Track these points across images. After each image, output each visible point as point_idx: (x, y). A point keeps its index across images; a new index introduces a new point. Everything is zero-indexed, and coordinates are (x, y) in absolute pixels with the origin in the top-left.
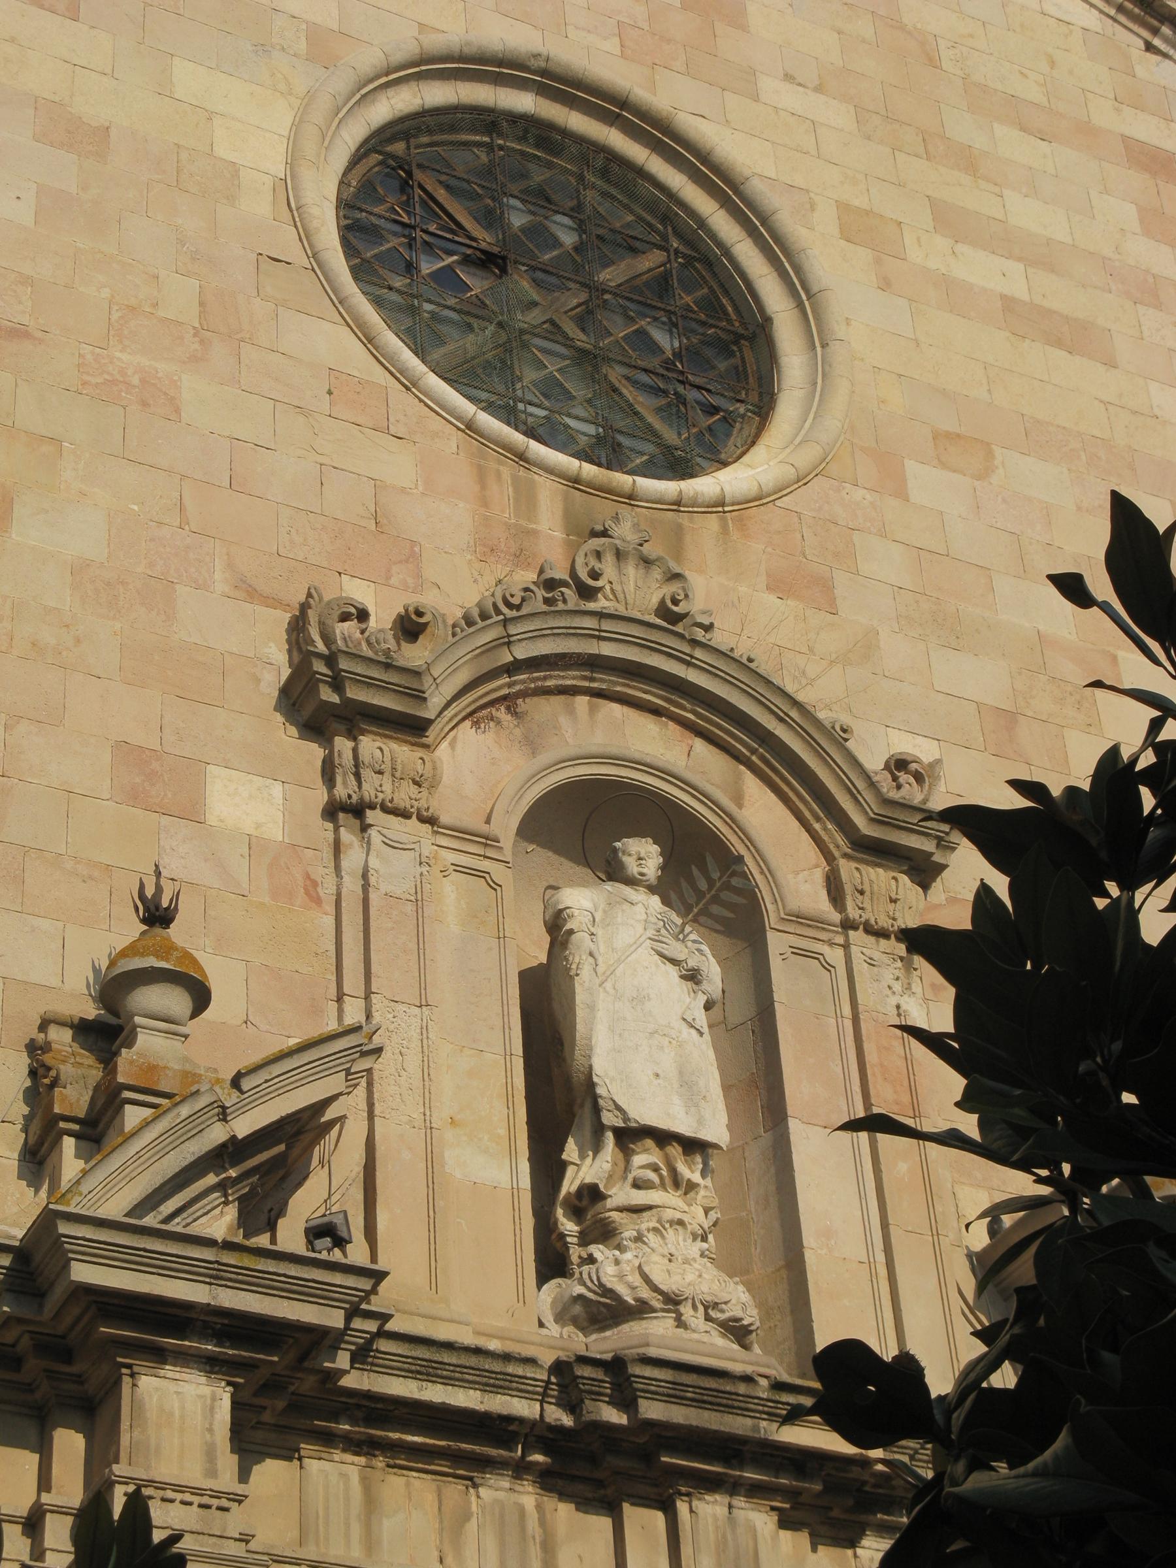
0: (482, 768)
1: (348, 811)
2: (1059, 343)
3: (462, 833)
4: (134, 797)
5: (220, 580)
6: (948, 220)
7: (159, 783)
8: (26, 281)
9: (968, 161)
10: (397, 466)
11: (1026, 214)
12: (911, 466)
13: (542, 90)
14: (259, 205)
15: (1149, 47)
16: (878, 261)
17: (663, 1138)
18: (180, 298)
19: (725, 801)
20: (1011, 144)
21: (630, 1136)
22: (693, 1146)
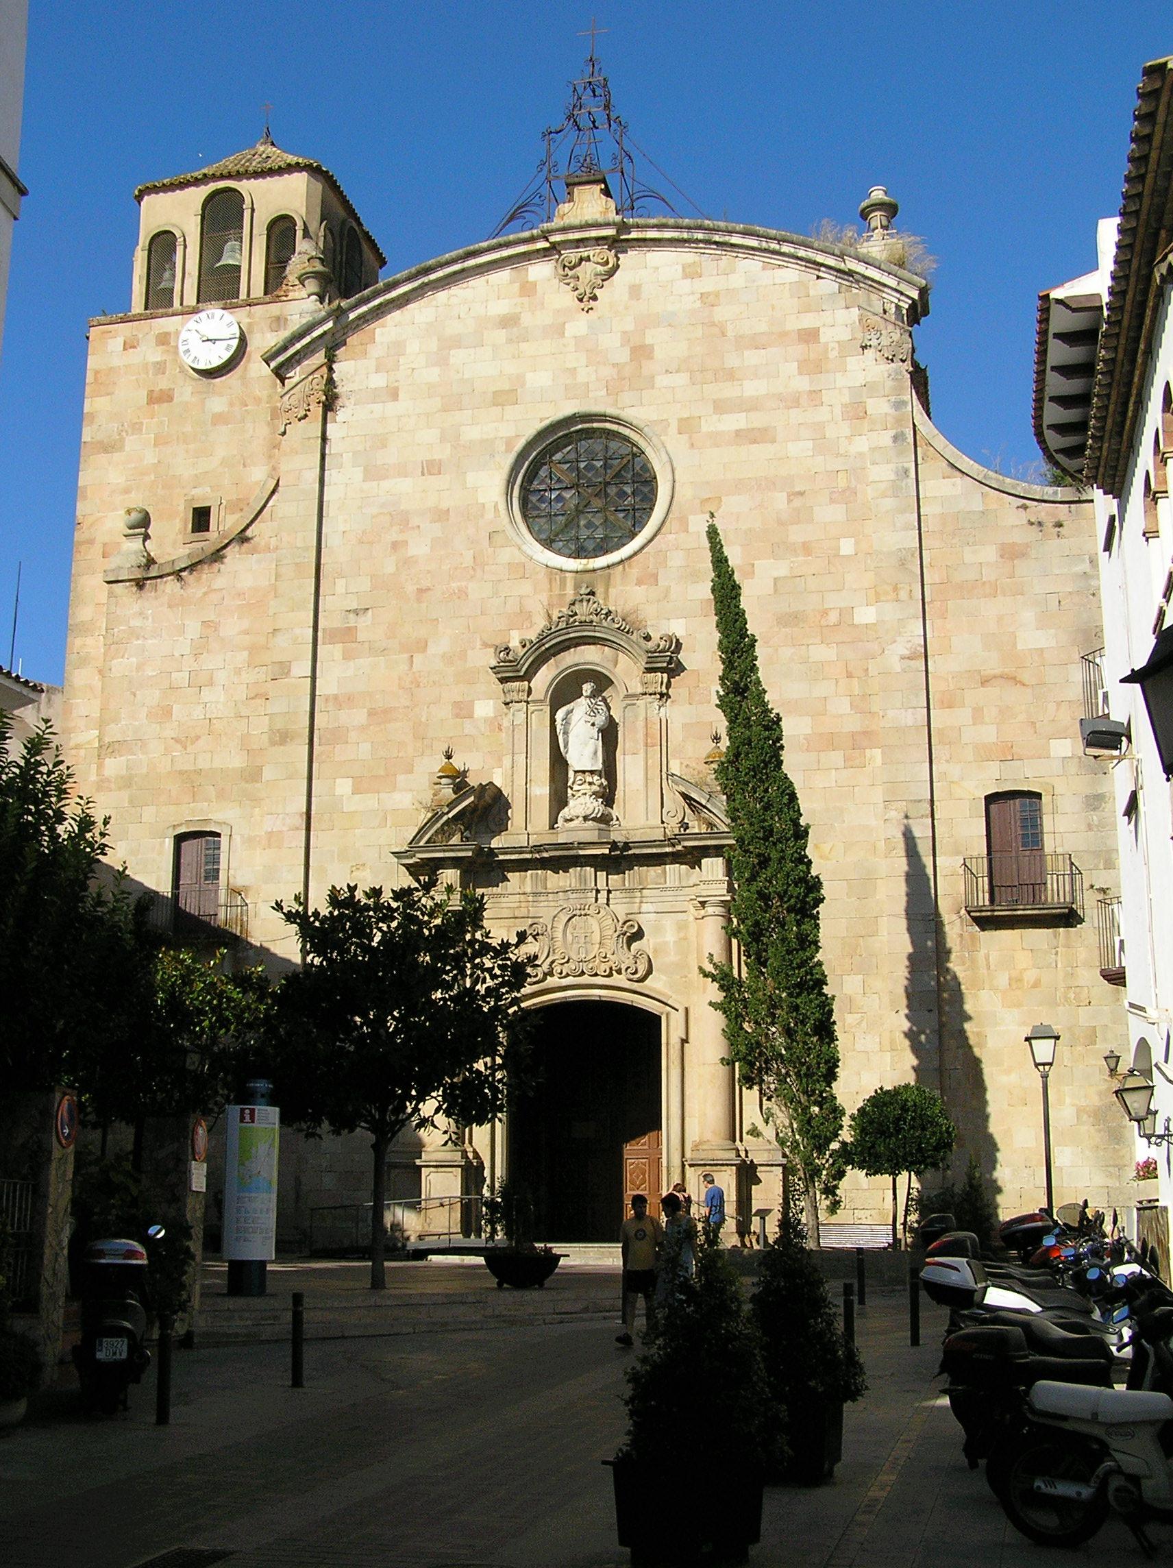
0: (544, 678)
1: (507, 704)
2: (755, 442)
3: (534, 701)
4: (457, 716)
5: (478, 644)
6: (720, 407)
7: (463, 711)
8: (429, 572)
9: (730, 375)
10: (526, 588)
11: (752, 388)
12: (691, 518)
13: (582, 422)
14: (490, 515)
15: (818, 277)
16: (690, 438)
17: (584, 772)
18: (468, 560)
19: (610, 666)
20: (753, 358)
21: (576, 772)
22: (592, 772)
